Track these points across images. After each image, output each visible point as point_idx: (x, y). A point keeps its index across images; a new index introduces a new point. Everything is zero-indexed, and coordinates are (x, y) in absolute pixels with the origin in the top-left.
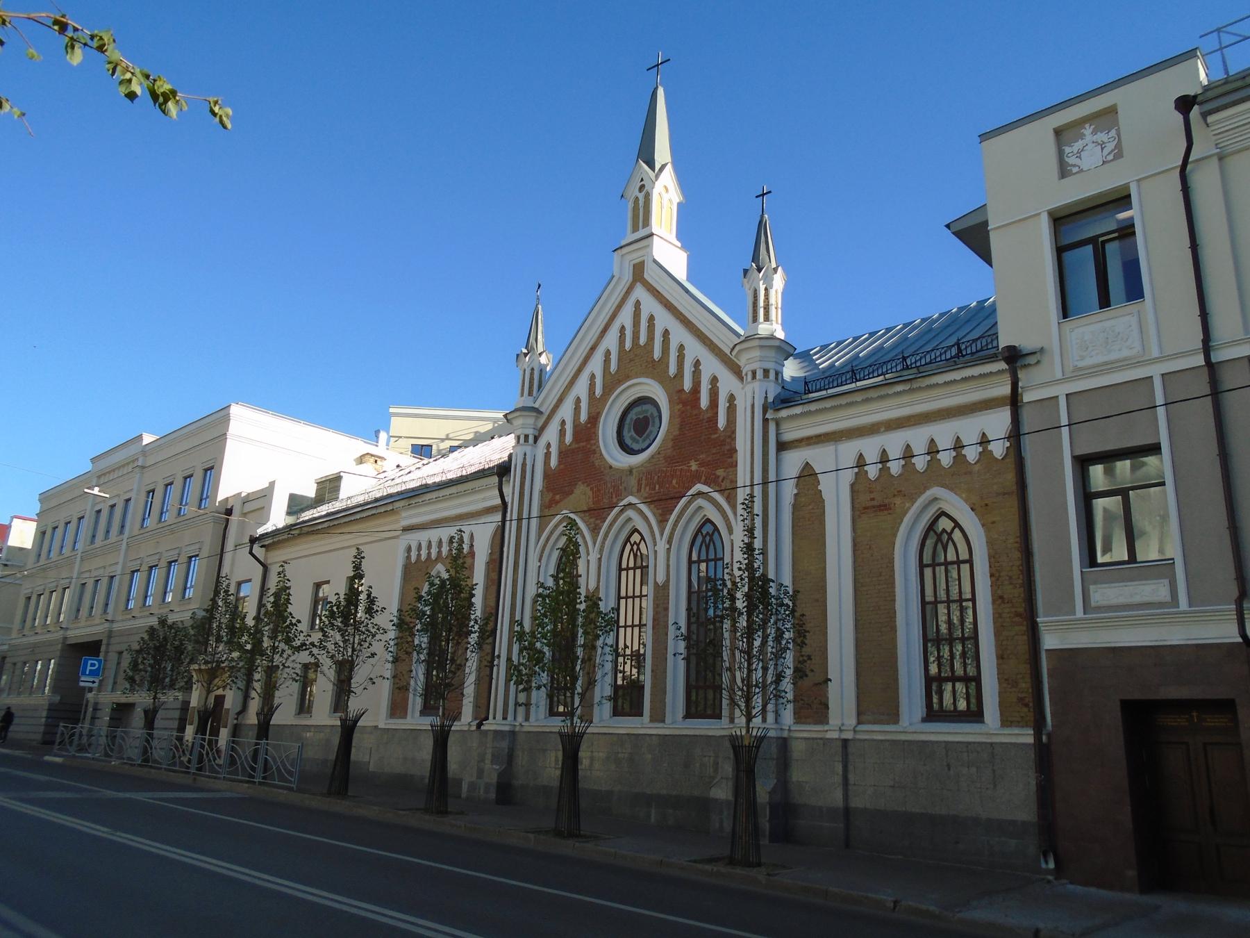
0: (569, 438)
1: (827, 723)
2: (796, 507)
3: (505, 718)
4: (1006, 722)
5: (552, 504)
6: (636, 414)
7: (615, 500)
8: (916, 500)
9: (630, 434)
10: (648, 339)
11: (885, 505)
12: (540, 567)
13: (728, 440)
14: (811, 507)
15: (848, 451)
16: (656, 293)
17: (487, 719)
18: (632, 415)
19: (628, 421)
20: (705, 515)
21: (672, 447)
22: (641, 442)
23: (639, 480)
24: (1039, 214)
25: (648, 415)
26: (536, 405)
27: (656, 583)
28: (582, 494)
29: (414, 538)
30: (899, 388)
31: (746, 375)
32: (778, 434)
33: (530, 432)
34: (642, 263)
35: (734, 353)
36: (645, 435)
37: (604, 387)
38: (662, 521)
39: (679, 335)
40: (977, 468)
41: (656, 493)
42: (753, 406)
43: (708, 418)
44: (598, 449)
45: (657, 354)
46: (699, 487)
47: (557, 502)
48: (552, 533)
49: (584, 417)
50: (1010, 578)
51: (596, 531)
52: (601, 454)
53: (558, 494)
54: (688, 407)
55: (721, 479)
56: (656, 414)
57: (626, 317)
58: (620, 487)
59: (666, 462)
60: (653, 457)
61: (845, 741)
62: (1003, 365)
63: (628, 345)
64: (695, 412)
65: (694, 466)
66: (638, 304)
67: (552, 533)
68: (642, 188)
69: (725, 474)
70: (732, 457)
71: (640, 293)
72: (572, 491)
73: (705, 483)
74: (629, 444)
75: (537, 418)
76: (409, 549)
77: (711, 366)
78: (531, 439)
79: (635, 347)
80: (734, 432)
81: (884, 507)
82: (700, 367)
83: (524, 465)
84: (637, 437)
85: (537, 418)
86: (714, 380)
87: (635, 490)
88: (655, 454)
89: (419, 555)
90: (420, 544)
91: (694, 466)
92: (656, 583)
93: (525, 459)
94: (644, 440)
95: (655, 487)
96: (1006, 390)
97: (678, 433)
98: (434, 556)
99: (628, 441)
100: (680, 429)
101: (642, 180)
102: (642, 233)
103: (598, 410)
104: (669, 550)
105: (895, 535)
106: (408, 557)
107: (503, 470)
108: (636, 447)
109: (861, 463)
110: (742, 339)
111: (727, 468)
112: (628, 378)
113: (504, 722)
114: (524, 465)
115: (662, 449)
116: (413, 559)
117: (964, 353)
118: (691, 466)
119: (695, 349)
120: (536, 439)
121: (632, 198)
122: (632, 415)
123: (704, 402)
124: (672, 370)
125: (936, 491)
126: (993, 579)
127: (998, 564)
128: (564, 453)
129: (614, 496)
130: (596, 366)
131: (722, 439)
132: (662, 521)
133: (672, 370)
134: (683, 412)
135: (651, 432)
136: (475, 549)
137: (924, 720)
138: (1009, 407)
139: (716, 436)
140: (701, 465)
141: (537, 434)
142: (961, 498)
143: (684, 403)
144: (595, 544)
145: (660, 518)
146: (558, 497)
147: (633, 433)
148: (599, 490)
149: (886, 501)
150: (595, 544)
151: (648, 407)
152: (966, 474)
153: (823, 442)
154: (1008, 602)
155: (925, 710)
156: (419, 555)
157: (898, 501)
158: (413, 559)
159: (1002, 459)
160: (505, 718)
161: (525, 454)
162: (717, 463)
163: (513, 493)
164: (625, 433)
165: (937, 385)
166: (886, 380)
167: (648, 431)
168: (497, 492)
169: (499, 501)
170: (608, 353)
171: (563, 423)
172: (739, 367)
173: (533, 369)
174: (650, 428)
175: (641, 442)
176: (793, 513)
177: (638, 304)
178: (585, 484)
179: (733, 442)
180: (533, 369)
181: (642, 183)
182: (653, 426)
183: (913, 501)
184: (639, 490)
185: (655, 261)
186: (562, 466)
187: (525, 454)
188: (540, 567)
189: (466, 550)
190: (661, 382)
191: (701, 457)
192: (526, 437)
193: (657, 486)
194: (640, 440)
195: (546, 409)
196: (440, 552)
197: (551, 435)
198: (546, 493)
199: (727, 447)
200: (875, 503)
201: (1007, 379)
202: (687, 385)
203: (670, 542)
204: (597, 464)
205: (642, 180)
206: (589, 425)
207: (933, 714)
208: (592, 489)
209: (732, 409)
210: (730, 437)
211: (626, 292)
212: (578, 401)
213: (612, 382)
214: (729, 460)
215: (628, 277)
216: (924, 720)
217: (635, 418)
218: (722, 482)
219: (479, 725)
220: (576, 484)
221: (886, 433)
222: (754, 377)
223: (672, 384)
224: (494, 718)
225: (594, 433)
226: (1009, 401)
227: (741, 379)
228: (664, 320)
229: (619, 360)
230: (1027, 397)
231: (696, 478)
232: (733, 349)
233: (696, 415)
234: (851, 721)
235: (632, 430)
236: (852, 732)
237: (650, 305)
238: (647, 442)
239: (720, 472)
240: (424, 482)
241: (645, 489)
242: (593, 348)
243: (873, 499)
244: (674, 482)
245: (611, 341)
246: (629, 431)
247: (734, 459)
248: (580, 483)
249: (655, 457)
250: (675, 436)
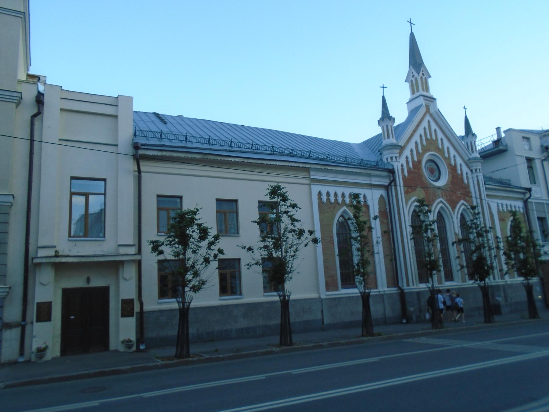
0: (411, 166)
6: (429, 165)
19: (426, 166)
24: (523, 156)
31: (476, 170)
37: (422, 150)
39: (446, 144)
45: (440, 146)
47: (410, 192)
49: (416, 159)
63: (429, 137)
66: (429, 122)
68: (423, 74)
71: (428, 118)
76: (320, 194)
87: (441, 196)
89: (328, 199)
94: (434, 177)
102: (425, 93)
123: (459, 172)
124: (447, 155)
128: (409, 171)
133: (447, 155)
146: (410, 190)
156: (328, 199)
173: (387, 126)
174: (435, 173)
180: (387, 126)
181: (423, 72)
182: (436, 172)
196: (344, 201)
202: (453, 163)
209: (468, 178)
210: (468, 187)
217: (429, 167)
228: (440, 135)
230: (529, 200)
244: (454, 197)
246: (428, 171)
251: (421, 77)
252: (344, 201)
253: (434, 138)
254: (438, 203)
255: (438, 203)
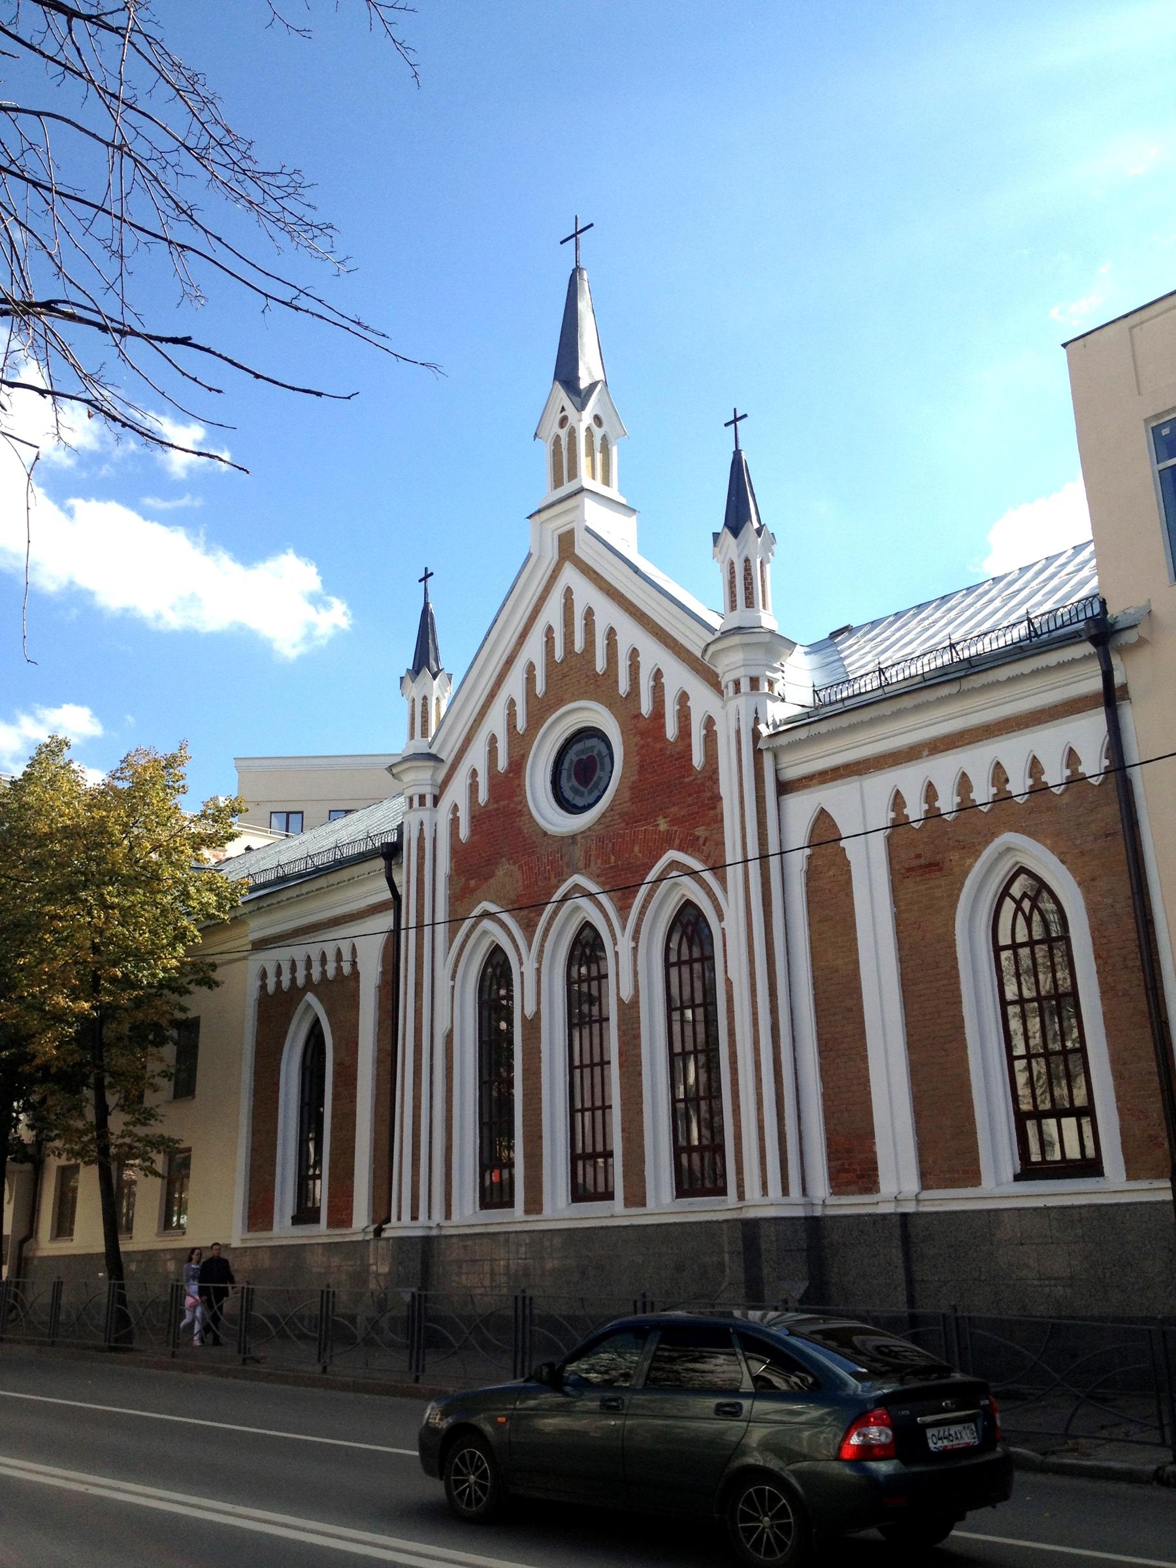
0: (483, 796)
1: (878, 1191)
2: (811, 874)
3: (414, 1218)
4: (1132, 1173)
5: (465, 893)
7: (554, 881)
8: (981, 853)
9: (570, 784)
10: (586, 643)
11: (938, 864)
12: (453, 987)
13: (709, 784)
14: (831, 873)
15: (880, 786)
16: (594, 576)
17: (388, 1220)
18: (572, 756)
19: (566, 765)
20: (683, 895)
21: (630, 799)
22: (586, 793)
23: (586, 852)
25: (595, 753)
26: (433, 751)
27: (619, 999)
28: (507, 874)
29: (268, 959)
30: (944, 691)
32: (777, 771)
33: (428, 791)
34: (571, 533)
35: (707, 657)
36: (592, 783)
37: (529, 716)
38: (623, 909)
39: (630, 635)
40: (1066, 799)
41: (611, 868)
42: (738, 732)
43: (678, 753)
44: (524, 809)
45: (600, 665)
46: (672, 855)
47: (472, 891)
48: (468, 936)
49: (502, 763)
50: (1125, 959)
51: (530, 929)
52: (531, 817)
53: (473, 878)
54: (649, 740)
55: (701, 841)
56: (605, 751)
57: (552, 613)
58: (560, 863)
59: (624, 820)
60: (603, 815)
61: (904, 1216)
62: (1088, 648)
63: (559, 654)
64: (658, 746)
65: (663, 826)
66: (568, 592)
67: (468, 936)
68: (563, 421)
69: (707, 834)
70: (714, 808)
71: (570, 576)
72: (494, 872)
73: (680, 849)
74: (570, 798)
75: (436, 769)
76: (264, 975)
77: (678, 677)
78: (429, 801)
79: (569, 656)
80: (715, 771)
81: (933, 866)
82: (663, 680)
83: (421, 839)
84: (582, 789)
85: (436, 769)
86: (683, 697)
87: (581, 864)
88: (606, 811)
90: (279, 967)
91: (663, 826)
92: (619, 999)
93: (421, 830)
94: (590, 792)
95: (609, 858)
96: (1095, 684)
97: (636, 777)
98: (301, 981)
99: (568, 794)
100: (640, 773)
101: (563, 409)
102: (568, 487)
103: (521, 752)
104: (635, 949)
105: (953, 906)
106: (263, 987)
107: (391, 852)
108: (579, 802)
109: (898, 801)
110: (718, 634)
111: (709, 824)
112: (561, 702)
113: (414, 1223)
114: (421, 839)
115: (618, 802)
116: (271, 988)
117: (1039, 633)
118: (658, 825)
119: (653, 655)
120: (436, 800)
121: (550, 438)
122: (572, 756)
123: (671, 730)
124: (623, 687)
125: (1008, 838)
126: (1100, 961)
127: (1105, 941)
128: (477, 818)
129: (552, 876)
130: (514, 686)
131: (699, 782)
132: (623, 909)
134: (642, 747)
135: (600, 778)
136: (360, 967)
137: (1017, 1178)
138: (1102, 709)
139: (692, 778)
140: (673, 822)
141: (437, 793)
142: (1045, 845)
143: (643, 734)
144: (530, 946)
145: (620, 903)
146: (473, 883)
147: (574, 782)
148: (531, 869)
149: (938, 857)
150: (530, 946)
151: (594, 742)
152: (1049, 809)
153: (842, 777)
154: (1123, 996)
155: (1018, 1162)
157: (955, 856)
158: (271, 988)
159: (1099, 785)
160: (414, 1218)
161: (422, 824)
162: (695, 818)
163: (408, 882)
164: (565, 784)
165: (997, 684)
166: (925, 681)
167: (595, 779)
168: (384, 883)
169: (388, 895)
170: (531, 667)
171: (474, 773)
172: (717, 676)
173: (425, 698)
174: (598, 773)
175: (586, 793)
176: (807, 885)
177: (568, 592)
178: (511, 862)
179: (715, 786)
182: (602, 769)
183: (977, 854)
184: (587, 865)
185: (588, 530)
186: (476, 837)
187: (422, 824)
188: (453, 987)
189: (347, 969)
190: (609, 706)
191: (672, 810)
192: (422, 798)
193: (613, 858)
194: (585, 791)
195: (448, 755)
196: (309, 977)
197: (457, 792)
198: (456, 878)
199: (709, 794)
200: (922, 861)
201: (1095, 668)
202: (646, 707)
203: (636, 937)
204: (525, 831)
205: (563, 409)
206: (511, 775)
207: (1028, 1171)
208: (520, 867)
209: (710, 737)
210: (710, 778)
211: (551, 577)
212: (493, 739)
213: (540, 710)
214: (712, 812)
215: (551, 553)
216: (1017, 1178)
217: (575, 759)
218: (704, 844)
219: (378, 1232)
220: (497, 863)
221: (931, 757)
222: (737, 690)
223: (625, 707)
224: (399, 1219)
225: (519, 785)
226: (1102, 700)
227: (721, 693)
228: (607, 614)
229: (548, 676)
231: (667, 842)
232: (705, 650)
233: (661, 750)
234: (911, 1184)
235: (573, 776)
236: (914, 1202)
237: (586, 595)
238: (596, 794)
239: (701, 831)
240: (281, 873)
241: (596, 864)
242: (509, 662)
243: (918, 856)
245: (534, 650)
247: (718, 811)
248: (504, 859)
249: (608, 814)
250: (633, 782)
251: (558, 439)
252: (309, 977)
253: (579, 645)
254: (565, 899)
255: (565, 899)
